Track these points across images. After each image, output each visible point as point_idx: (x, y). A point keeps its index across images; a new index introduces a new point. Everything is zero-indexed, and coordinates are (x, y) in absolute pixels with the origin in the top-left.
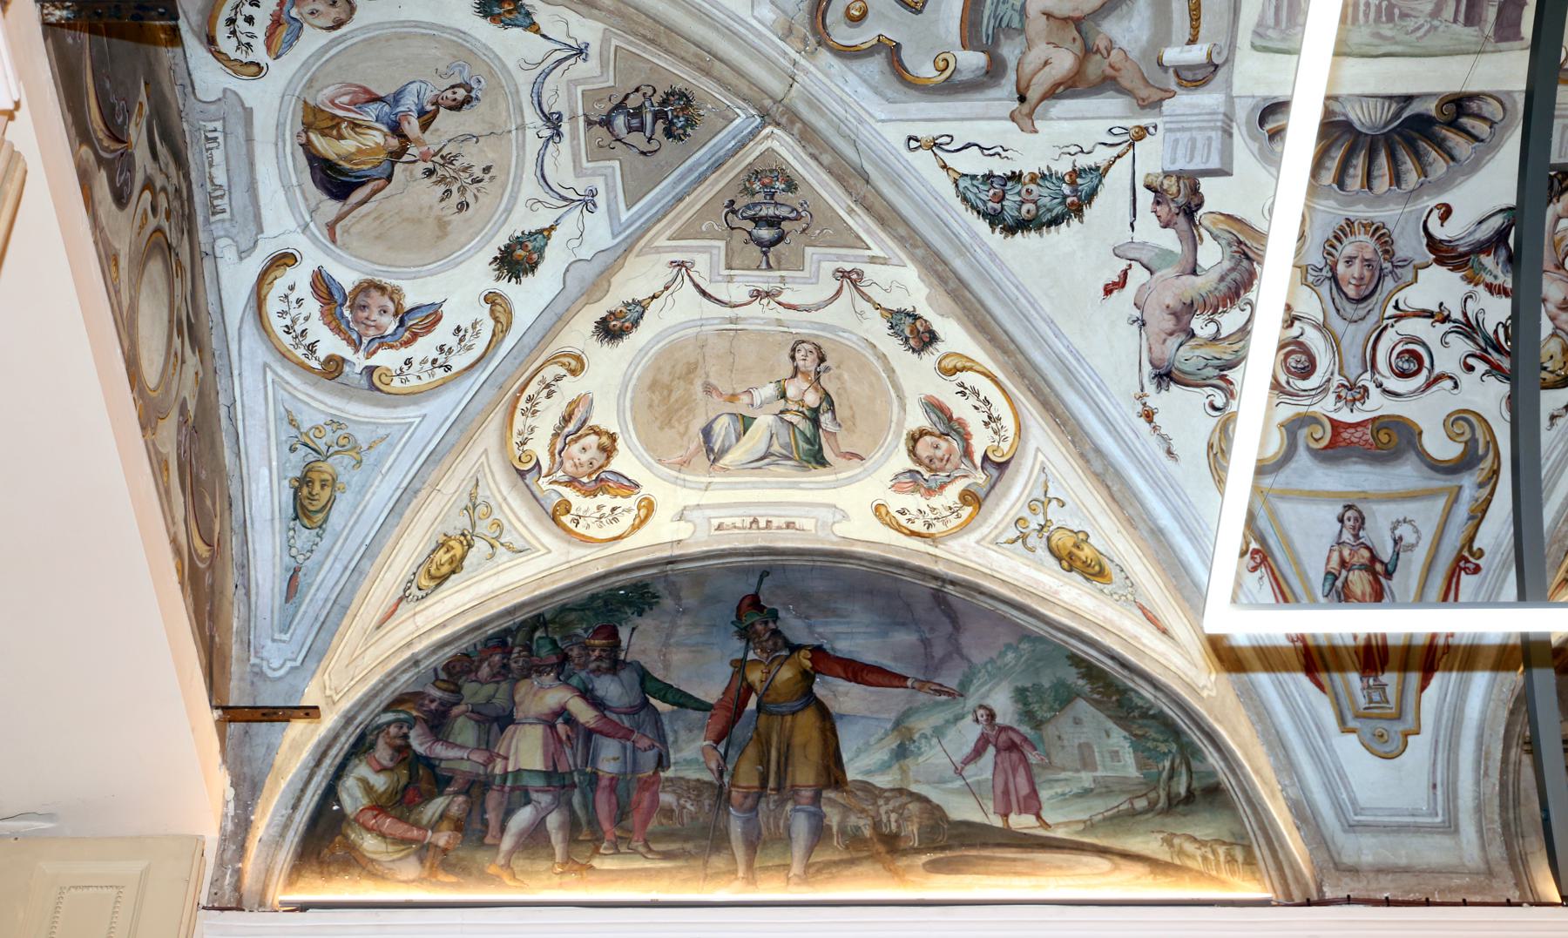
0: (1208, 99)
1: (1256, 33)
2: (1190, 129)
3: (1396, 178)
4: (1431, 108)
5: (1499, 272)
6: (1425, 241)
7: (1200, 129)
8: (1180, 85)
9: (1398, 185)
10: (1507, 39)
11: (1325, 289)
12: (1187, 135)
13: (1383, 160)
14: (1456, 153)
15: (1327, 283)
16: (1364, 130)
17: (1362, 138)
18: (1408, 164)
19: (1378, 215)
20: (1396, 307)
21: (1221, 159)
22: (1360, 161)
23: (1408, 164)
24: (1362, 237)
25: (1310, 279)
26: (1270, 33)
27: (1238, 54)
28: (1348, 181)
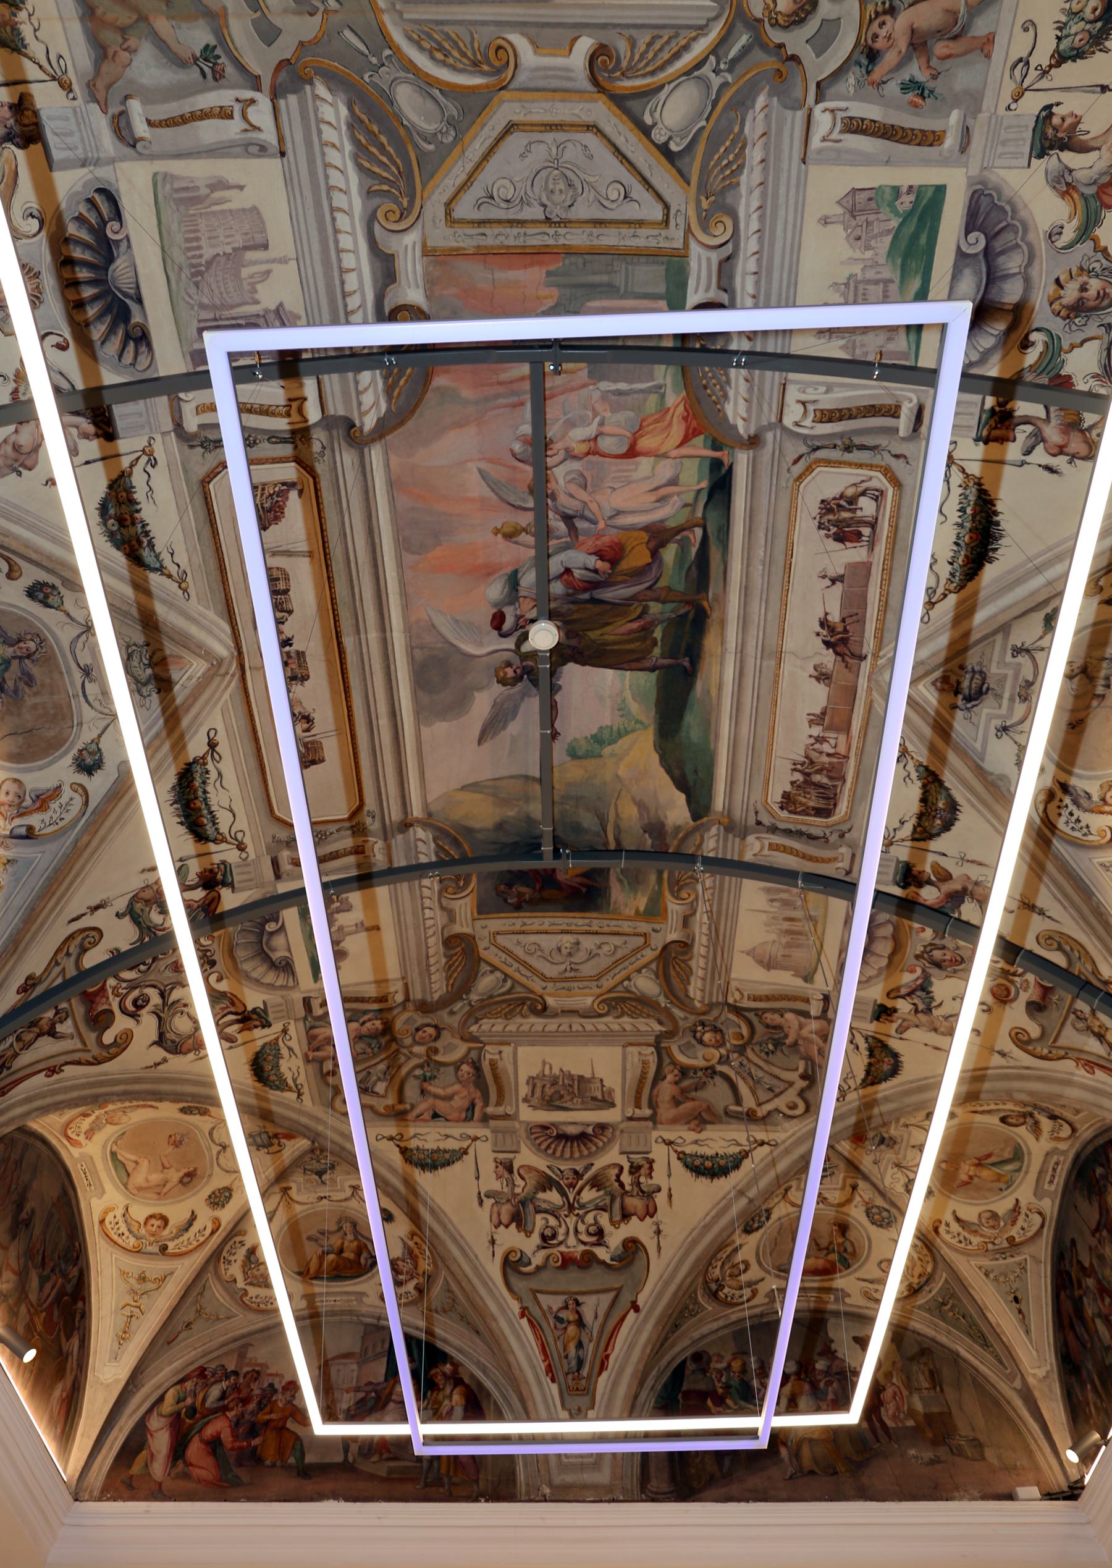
0: (108, 143)
1: (166, 175)
2: (80, 130)
4: (136, 318)
7: (82, 139)
8: (113, 117)
10: (192, 359)
12: (75, 128)
14: (108, 344)
21: (63, 160)
26: (168, 186)
27: (147, 163)
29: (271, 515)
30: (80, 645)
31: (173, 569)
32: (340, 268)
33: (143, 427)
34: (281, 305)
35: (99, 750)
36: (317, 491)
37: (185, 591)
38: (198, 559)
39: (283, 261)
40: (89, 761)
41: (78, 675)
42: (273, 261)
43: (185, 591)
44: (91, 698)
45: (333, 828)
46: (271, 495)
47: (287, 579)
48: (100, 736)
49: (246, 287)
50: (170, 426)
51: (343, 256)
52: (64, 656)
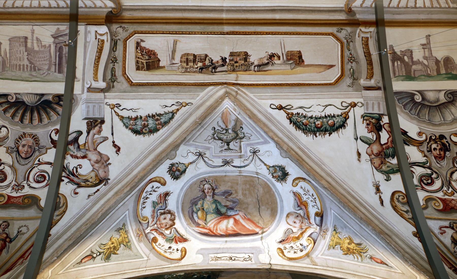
3: (41, 120)
5: (75, 151)
6: (50, 140)
9: (41, 122)
11: (14, 155)
13: (36, 114)
15: (15, 153)
16: (29, 104)
17: (28, 107)
18: (44, 116)
19: (34, 132)
20: (39, 161)
22: (28, 115)
23: (44, 116)
24: (29, 139)
25: (9, 151)
28: (24, 121)
29: (152, 57)
30: (210, 162)
31: (174, 108)
32: (38, 7)
33: (100, 106)
34: (52, 35)
35: (273, 167)
36: (142, 33)
37: (187, 104)
38: (171, 95)
39: (33, 32)
40: (280, 174)
41: (227, 168)
42: (33, 36)
43: (187, 104)
44: (243, 164)
45: (347, 53)
46: (142, 55)
47: (188, 54)
48: (265, 165)
49: (43, 49)
50: (102, 95)
51: (33, 6)
52: (216, 172)
